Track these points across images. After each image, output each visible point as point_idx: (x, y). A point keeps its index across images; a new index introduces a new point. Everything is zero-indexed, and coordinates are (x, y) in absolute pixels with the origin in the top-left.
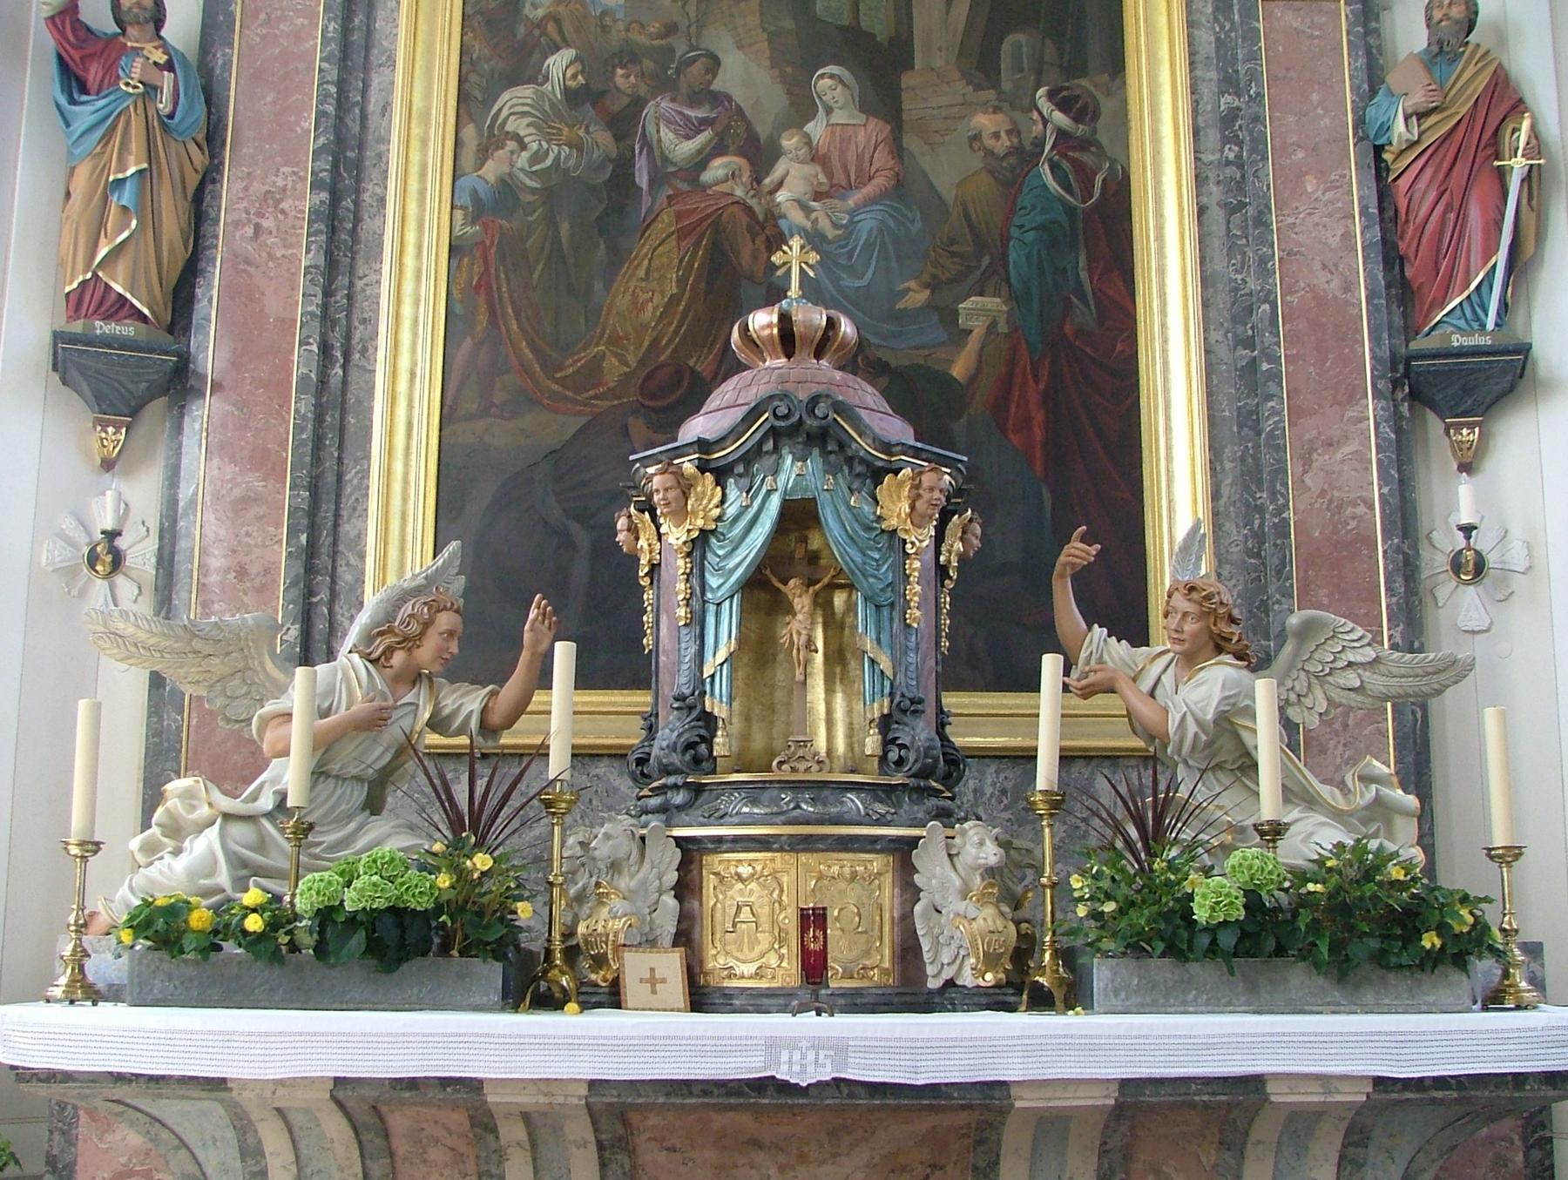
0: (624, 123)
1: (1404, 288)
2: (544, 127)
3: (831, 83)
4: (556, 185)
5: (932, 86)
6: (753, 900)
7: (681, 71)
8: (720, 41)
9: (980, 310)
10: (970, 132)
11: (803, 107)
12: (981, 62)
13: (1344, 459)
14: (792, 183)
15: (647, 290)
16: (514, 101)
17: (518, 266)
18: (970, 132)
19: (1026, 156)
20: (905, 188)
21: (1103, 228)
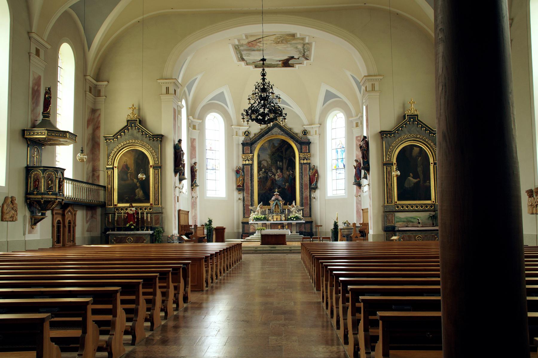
0: (267, 173)
1: (311, 183)
2: (263, 173)
3: (279, 171)
4: (263, 177)
5: (285, 170)
6: (275, 217)
7: (270, 170)
9: (287, 184)
11: (277, 172)
12: (287, 169)
14: (277, 177)
15: (269, 183)
17: (261, 182)
19: (290, 175)
20: (283, 177)
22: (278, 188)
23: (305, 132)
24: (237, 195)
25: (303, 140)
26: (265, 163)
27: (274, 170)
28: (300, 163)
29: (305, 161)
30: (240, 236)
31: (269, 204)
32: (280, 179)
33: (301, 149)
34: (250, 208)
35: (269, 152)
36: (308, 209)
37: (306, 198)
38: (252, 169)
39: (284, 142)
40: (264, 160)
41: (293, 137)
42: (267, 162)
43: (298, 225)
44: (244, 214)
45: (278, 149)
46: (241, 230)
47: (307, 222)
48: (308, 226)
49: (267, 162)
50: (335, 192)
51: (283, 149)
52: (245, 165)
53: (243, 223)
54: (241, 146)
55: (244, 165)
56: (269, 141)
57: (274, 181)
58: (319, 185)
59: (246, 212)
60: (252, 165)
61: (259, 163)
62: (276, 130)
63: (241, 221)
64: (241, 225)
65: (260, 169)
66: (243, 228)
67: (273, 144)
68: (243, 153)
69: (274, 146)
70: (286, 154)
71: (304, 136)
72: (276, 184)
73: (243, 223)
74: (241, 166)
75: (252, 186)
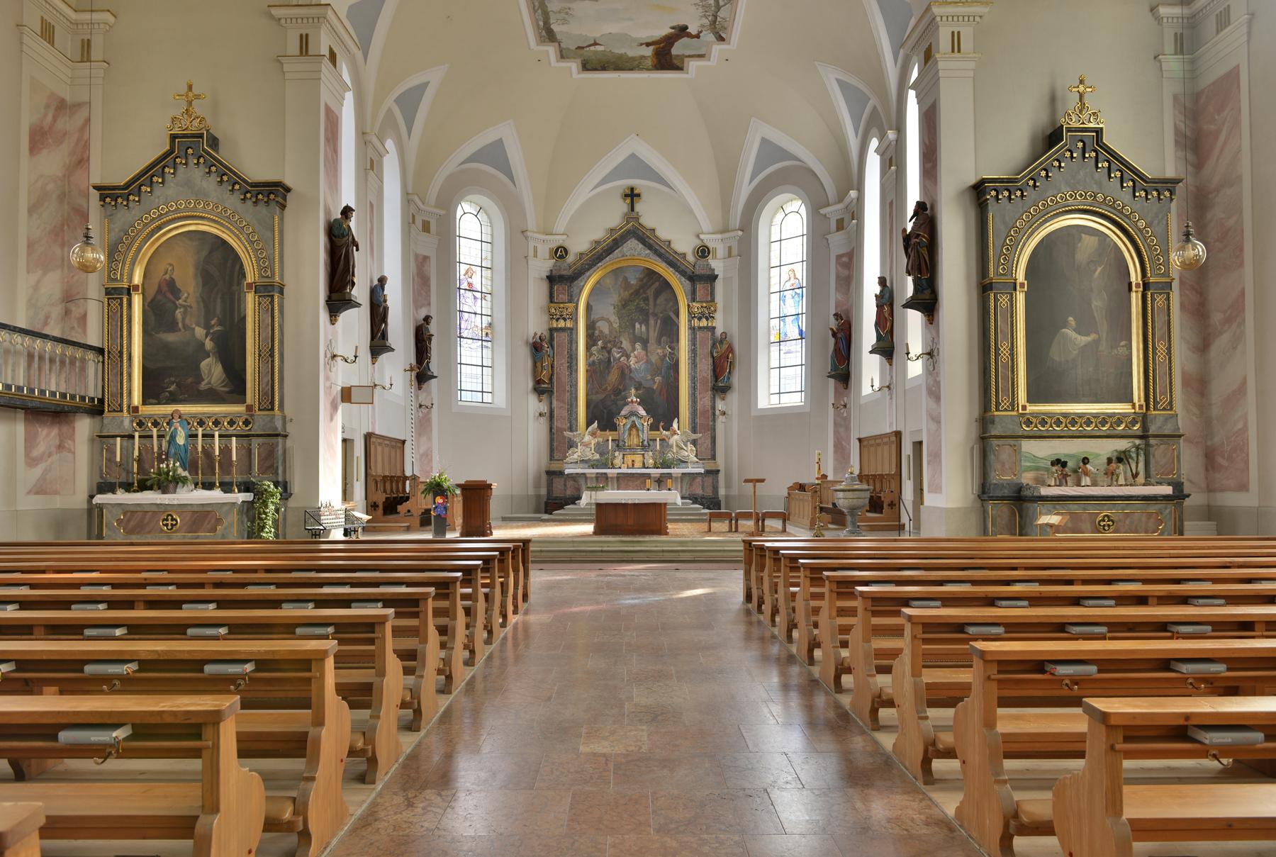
0: (609, 352)
3: (638, 346)
4: (600, 361)
5: (652, 345)
8: (622, 339)
9: (658, 379)
10: (657, 352)
11: (634, 349)
12: (659, 342)
13: (705, 400)
14: (632, 361)
15: (613, 377)
16: (594, 348)
18: (657, 352)
19: (665, 356)
21: (675, 367)
22: (637, 389)
23: (703, 251)
24: (534, 405)
25: (698, 271)
26: (603, 327)
27: (626, 344)
28: (693, 329)
29: (704, 323)
30: (543, 506)
31: (614, 428)
32: (642, 365)
33: (694, 292)
34: (567, 434)
35: (614, 298)
36: (708, 441)
37: (704, 413)
38: (573, 342)
39: (651, 275)
40: (602, 319)
41: (673, 261)
42: (611, 324)
43: (687, 479)
44: (552, 450)
45: (637, 293)
46: (544, 491)
47: (708, 472)
48: (709, 480)
49: (611, 324)
50: (775, 400)
51: (650, 292)
52: (557, 330)
53: (548, 473)
54: (545, 286)
55: (551, 330)
56: (616, 272)
57: (627, 371)
58: (736, 380)
59: (558, 444)
60: (572, 331)
61: (590, 327)
62: (632, 245)
63: (544, 469)
64: (544, 477)
65: (591, 340)
66: (550, 485)
67: (626, 279)
68: (552, 301)
69: (627, 285)
70: (655, 305)
71: (701, 262)
72: (631, 378)
73: (548, 473)
74: (546, 334)
75: (574, 385)
